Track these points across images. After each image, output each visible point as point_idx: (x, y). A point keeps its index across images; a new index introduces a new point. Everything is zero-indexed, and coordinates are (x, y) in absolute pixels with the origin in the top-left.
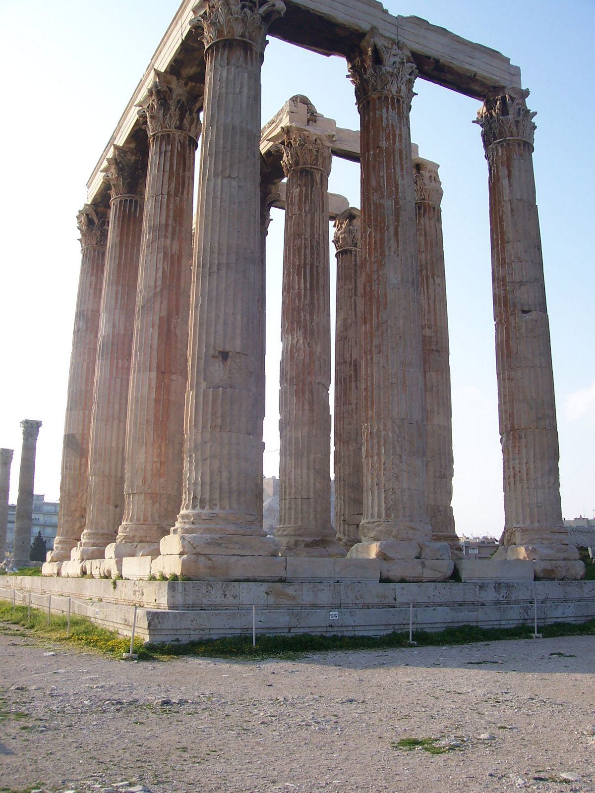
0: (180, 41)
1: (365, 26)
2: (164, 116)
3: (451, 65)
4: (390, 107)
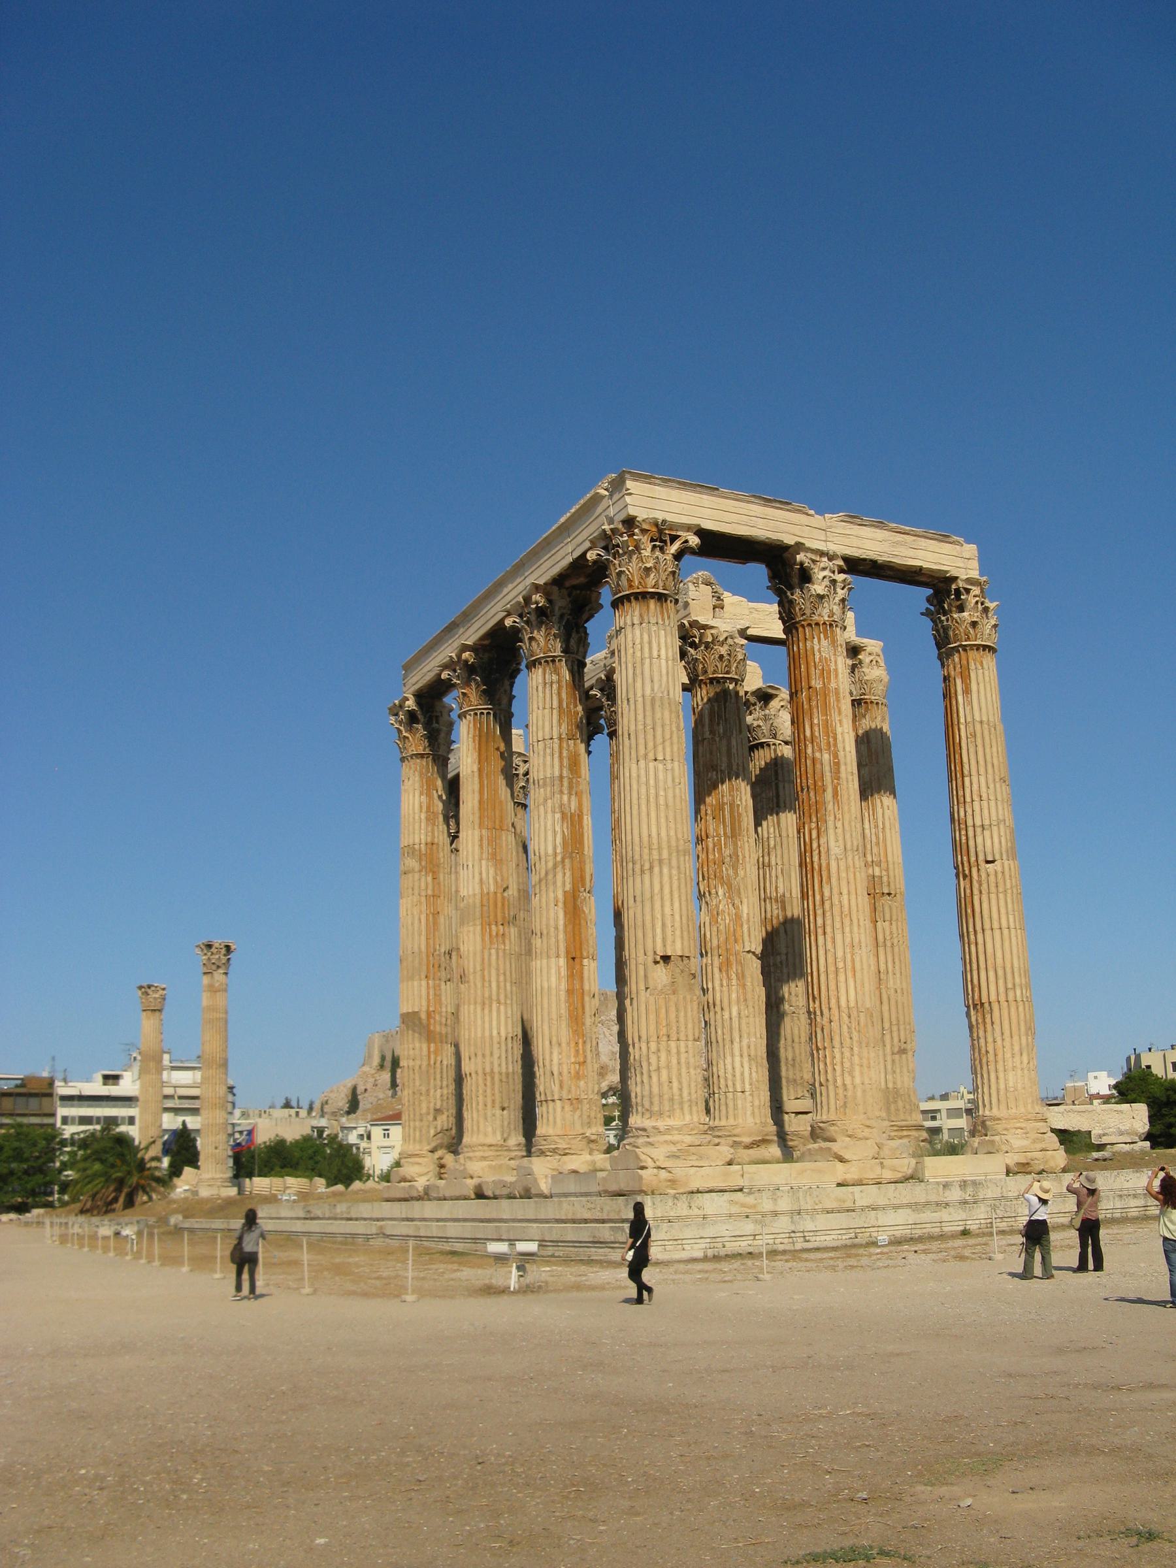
0: (570, 559)
1: (790, 540)
2: (546, 637)
4: (822, 635)
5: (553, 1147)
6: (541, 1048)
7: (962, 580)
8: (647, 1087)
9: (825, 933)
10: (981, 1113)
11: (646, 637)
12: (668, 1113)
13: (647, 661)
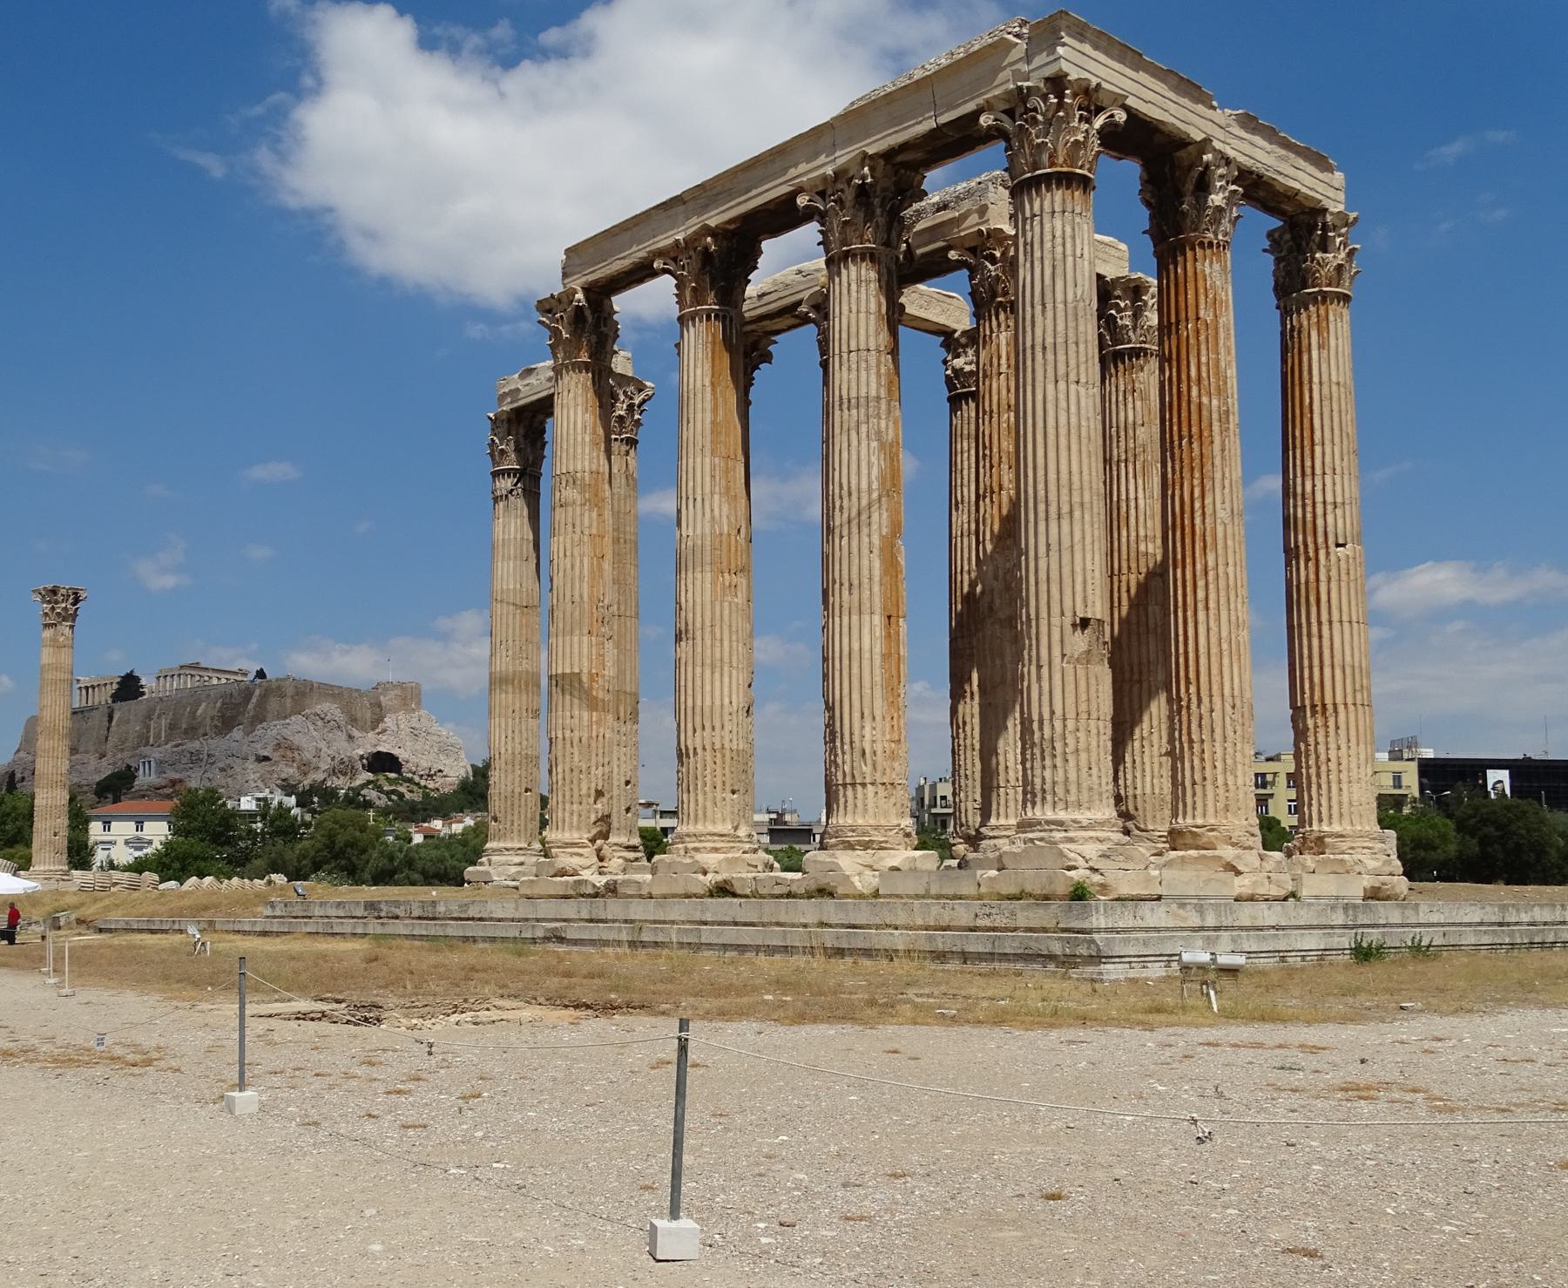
3: (1275, 183)
5: (867, 839)
6: (849, 719)
7: (1332, 214)
8: (1060, 772)
9: (1207, 608)
10: (1315, 827)
11: (1068, 230)
12: (1087, 805)
13: (1070, 259)
